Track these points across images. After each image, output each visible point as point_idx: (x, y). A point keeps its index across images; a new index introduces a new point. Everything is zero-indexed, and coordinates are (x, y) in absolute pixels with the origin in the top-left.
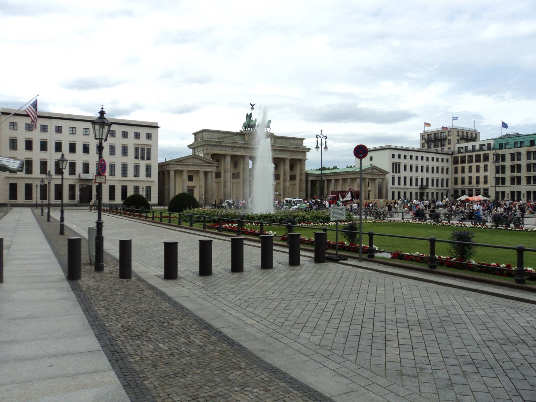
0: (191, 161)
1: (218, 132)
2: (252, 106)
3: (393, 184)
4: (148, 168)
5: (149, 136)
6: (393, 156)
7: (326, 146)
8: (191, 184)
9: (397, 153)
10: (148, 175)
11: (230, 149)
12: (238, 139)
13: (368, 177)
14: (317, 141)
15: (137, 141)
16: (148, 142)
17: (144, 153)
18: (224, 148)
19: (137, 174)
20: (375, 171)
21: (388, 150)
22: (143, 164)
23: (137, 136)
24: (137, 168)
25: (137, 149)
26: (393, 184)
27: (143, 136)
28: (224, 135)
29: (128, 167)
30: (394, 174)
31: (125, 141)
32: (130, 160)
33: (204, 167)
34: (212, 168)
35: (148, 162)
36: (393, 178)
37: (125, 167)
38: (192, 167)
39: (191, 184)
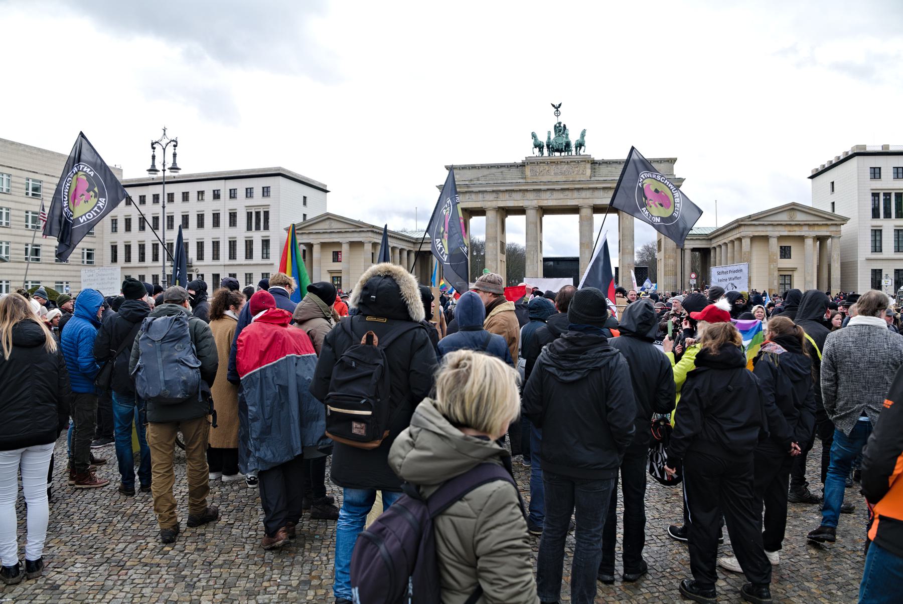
1: (473, 167)
2: (557, 108)
3: (877, 247)
4: (266, 243)
5: (266, 191)
6: (876, 173)
7: (174, 163)
8: (336, 266)
9: (887, 165)
10: (266, 255)
11: (491, 197)
12: (513, 177)
13: (778, 234)
14: (154, 157)
15: (250, 202)
16: (265, 201)
17: (259, 219)
18: (480, 195)
19: (249, 254)
20: (800, 217)
21: (856, 158)
22: (257, 237)
23: (249, 193)
24: (249, 244)
25: (249, 215)
26: (877, 247)
27: (257, 192)
28: (485, 172)
29: (238, 244)
30: (881, 222)
31: (233, 204)
32: (240, 233)
33: (348, 235)
34: (363, 235)
35: (266, 233)
36: (877, 233)
37: (233, 245)
38: (326, 236)
39: (336, 266)
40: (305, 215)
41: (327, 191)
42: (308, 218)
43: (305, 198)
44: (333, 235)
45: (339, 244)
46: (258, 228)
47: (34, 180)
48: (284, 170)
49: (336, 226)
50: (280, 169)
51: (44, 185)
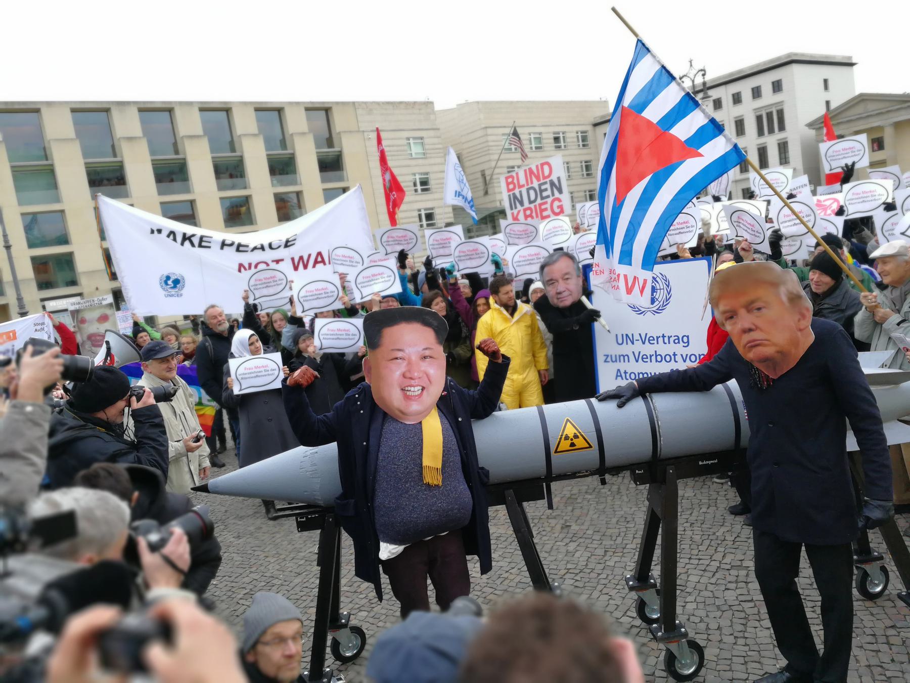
0: (859, 110)
4: (783, 147)
5: (777, 87)
15: (759, 103)
17: (772, 121)
22: (771, 142)
23: (757, 93)
24: (762, 153)
25: (759, 119)
27: (767, 89)
31: (738, 111)
33: (891, 115)
38: (861, 122)
40: (828, 103)
41: (851, 65)
42: (833, 106)
43: (826, 81)
44: (871, 120)
45: (880, 128)
46: (771, 131)
47: (534, 133)
48: (796, 54)
49: (872, 107)
50: (789, 55)
51: (544, 136)
